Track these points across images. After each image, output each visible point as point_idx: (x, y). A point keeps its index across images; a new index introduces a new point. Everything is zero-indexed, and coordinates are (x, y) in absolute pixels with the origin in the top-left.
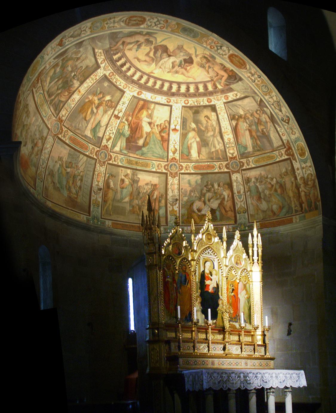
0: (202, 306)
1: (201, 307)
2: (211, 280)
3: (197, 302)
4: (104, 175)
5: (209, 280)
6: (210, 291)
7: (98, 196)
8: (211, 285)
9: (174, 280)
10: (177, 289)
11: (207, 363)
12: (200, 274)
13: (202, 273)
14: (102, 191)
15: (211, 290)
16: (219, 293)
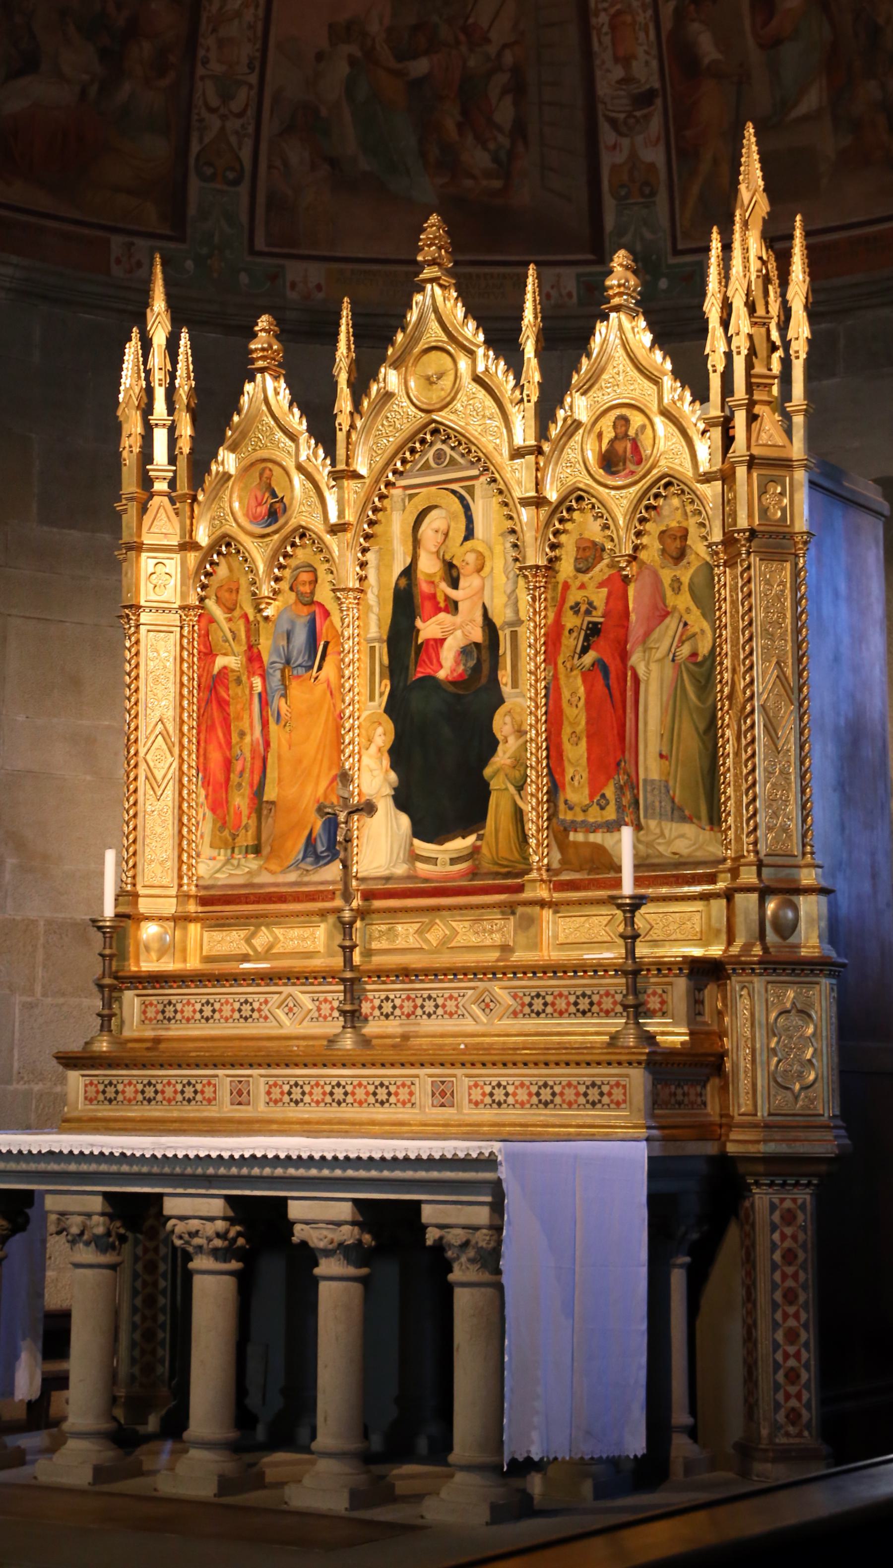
0: (394, 766)
1: (393, 776)
2: (453, 607)
3: (373, 749)
4: (650, 12)
5: (438, 610)
6: (442, 674)
7: (639, 139)
8: (448, 637)
9: (253, 657)
10: (264, 701)
11: (209, 1091)
12: (389, 595)
13: (403, 582)
14: (659, 102)
15: (448, 665)
16: (500, 674)
